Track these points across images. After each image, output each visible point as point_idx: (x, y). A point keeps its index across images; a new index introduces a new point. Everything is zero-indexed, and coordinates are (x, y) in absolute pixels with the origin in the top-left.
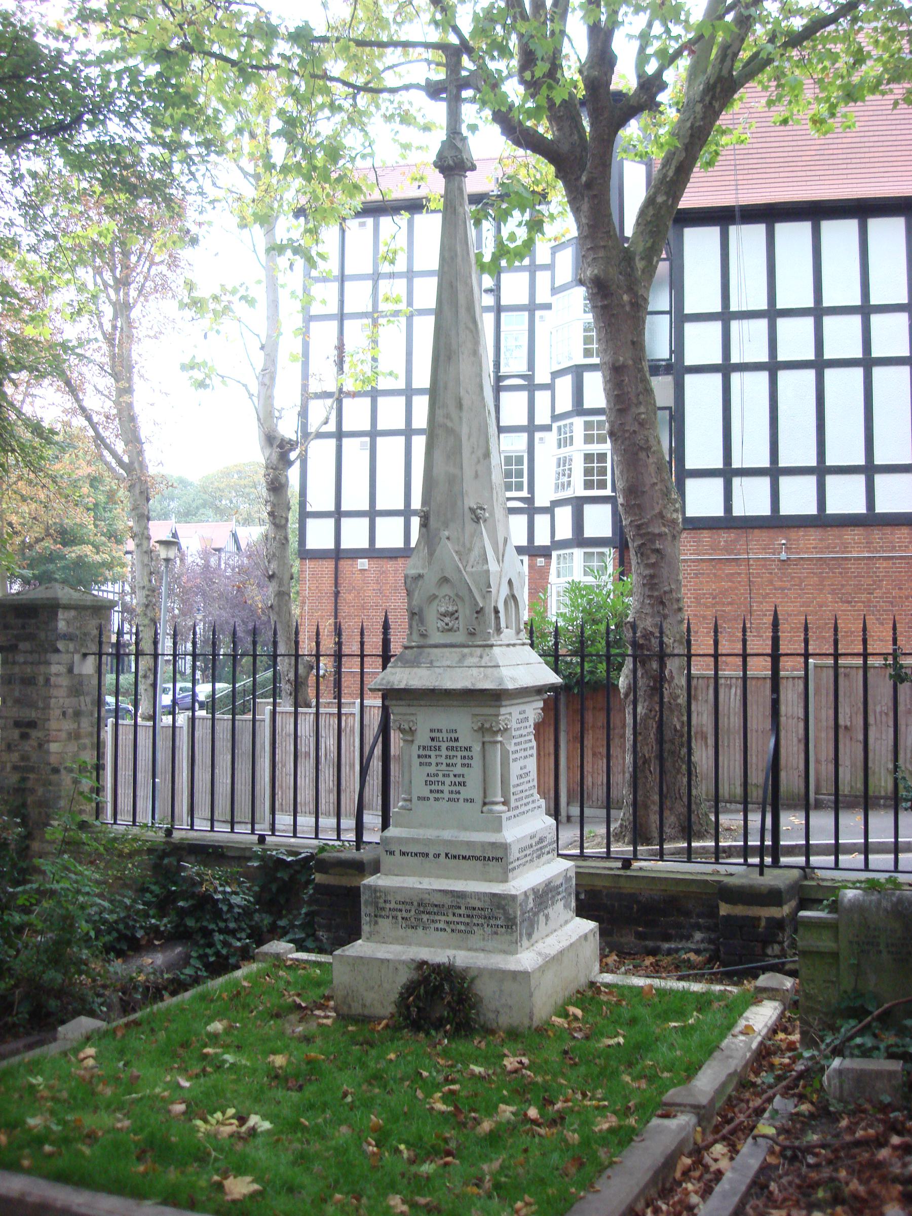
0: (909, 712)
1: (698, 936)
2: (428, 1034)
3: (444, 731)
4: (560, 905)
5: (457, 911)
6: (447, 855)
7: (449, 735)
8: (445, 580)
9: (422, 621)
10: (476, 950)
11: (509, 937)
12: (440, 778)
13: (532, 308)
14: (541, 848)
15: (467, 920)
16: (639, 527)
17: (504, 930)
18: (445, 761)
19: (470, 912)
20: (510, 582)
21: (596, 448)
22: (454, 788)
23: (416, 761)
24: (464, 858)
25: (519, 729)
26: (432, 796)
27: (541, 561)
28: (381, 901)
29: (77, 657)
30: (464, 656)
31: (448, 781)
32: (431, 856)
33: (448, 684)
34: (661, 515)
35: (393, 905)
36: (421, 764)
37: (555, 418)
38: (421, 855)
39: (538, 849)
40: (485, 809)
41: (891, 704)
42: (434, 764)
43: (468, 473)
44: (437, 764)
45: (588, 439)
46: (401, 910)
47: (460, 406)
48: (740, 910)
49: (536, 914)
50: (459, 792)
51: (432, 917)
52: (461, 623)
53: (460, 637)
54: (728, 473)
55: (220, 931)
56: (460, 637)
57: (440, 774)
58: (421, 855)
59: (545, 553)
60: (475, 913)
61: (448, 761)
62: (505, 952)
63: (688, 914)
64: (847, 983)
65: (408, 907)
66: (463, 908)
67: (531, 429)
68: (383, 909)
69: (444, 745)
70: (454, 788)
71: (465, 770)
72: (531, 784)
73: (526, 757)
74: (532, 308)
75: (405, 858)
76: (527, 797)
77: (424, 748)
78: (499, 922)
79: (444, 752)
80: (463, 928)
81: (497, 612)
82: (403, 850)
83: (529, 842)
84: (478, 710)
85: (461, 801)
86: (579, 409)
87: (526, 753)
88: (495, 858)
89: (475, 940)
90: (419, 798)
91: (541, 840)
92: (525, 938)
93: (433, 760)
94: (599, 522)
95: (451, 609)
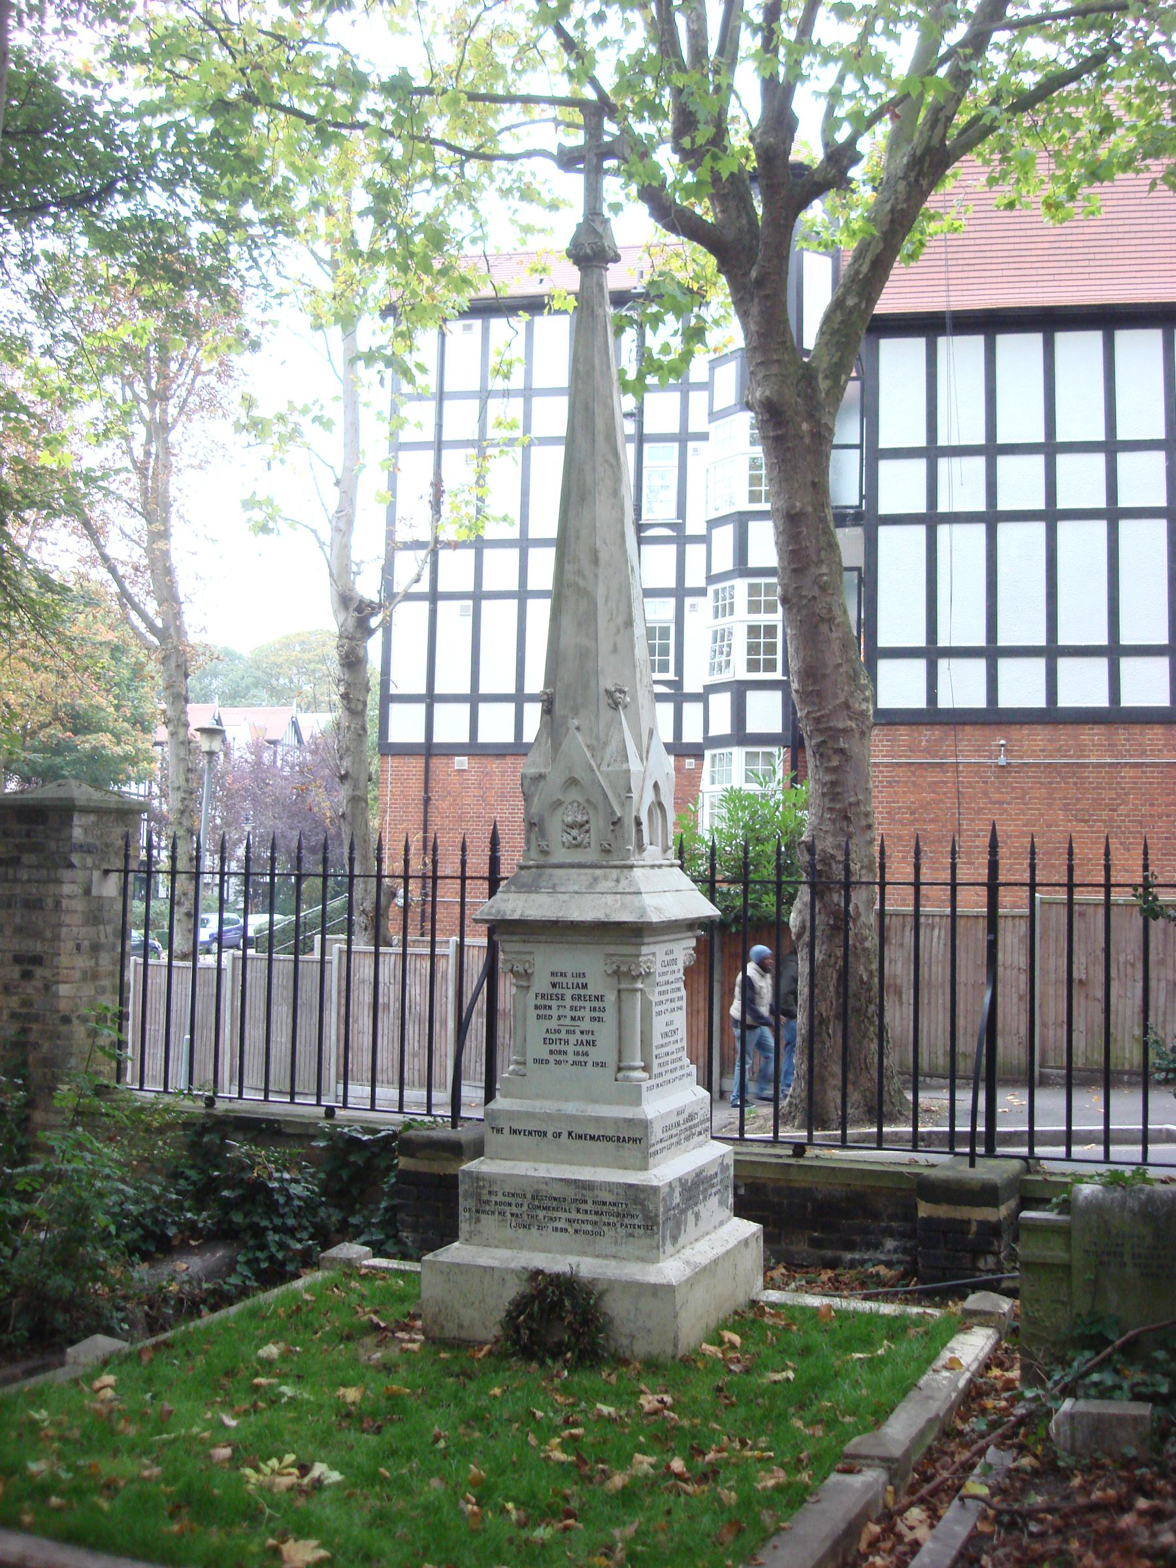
0: (1162, 962)
1: (890, 1244)
2: (542, 1363)
4: (714, 1201)
5: (583, 1207)
6: (570, 1134)
7: (575, 981)
8: (572, 782)
9: (542, 833)
10: (606, 1257)
11: (649, 1241)
12: (563, 1035)
13: (683, 438)
14: (691, 1128)
15: (595, 1218)
16: (818, 720)
17: (642, 1231)
18: (569, 1014)
19: (599, 1208)
20: (656, 786)
21: (763, 619)
22: (580, 1049)
23: (532, 1013)
24: (592, 1138)
25: (664, 974)
26: (552, 1058)
27: (690, 763)
28: (485, 1192)
29: (96, 875)
30: (596, 879)
31: (572, 1039)
32: (549, 1135)
33: (576, 915)
34: (847, 706)
36: (539, 1017)
37: (711, 579)
38: (537, 1134)
39: (687, 1128)
40: (620, 1075)
41: (1139, 953)
43: (604, 646)
44: (559, 1018)
45: (754, 607)
46: (510, 1204)
47: (596, 561)
48: (943, 1211)
49: (683, 1212)
50: (587, 1054)
52: (593, 838)
53: (590, 855)
54: (932, 653)
55: (276, 1230)
56: (590, 855)
57: (564, 1030)
58: (537, 1134)
59: (696, 751)
60: (605, 1208)
61: (574, 1013)
62: (643, 1260)
63: (876, 1216)
64: (1082, 1304)
65: (520, 1201)
66: (590, 1202)
67: (680, 592)
68: (488, 1202)
69: (569, 993)
70: (580, 1049)
71: (595, 1026)
72: (679, 1045)
73: (673, 1010)
74: (683, 438)
76: (673, 1061)
77: (543, 996)
78: (636, 1222)
79: (568, 1002)
80: (589, 1228)
81: (638, 823)
83: (674, 1119)
84: (612, 949)
85: (590, 1064)
86: (742, 568)
87: (674, 1005)
88: (632, 1139)
89: (604, 1243)
90: (536, 1061)
91: (691, 1117)
92: (668, 1242)
93: (554, 1013)
94: (766, 713)
95: (580, 818)
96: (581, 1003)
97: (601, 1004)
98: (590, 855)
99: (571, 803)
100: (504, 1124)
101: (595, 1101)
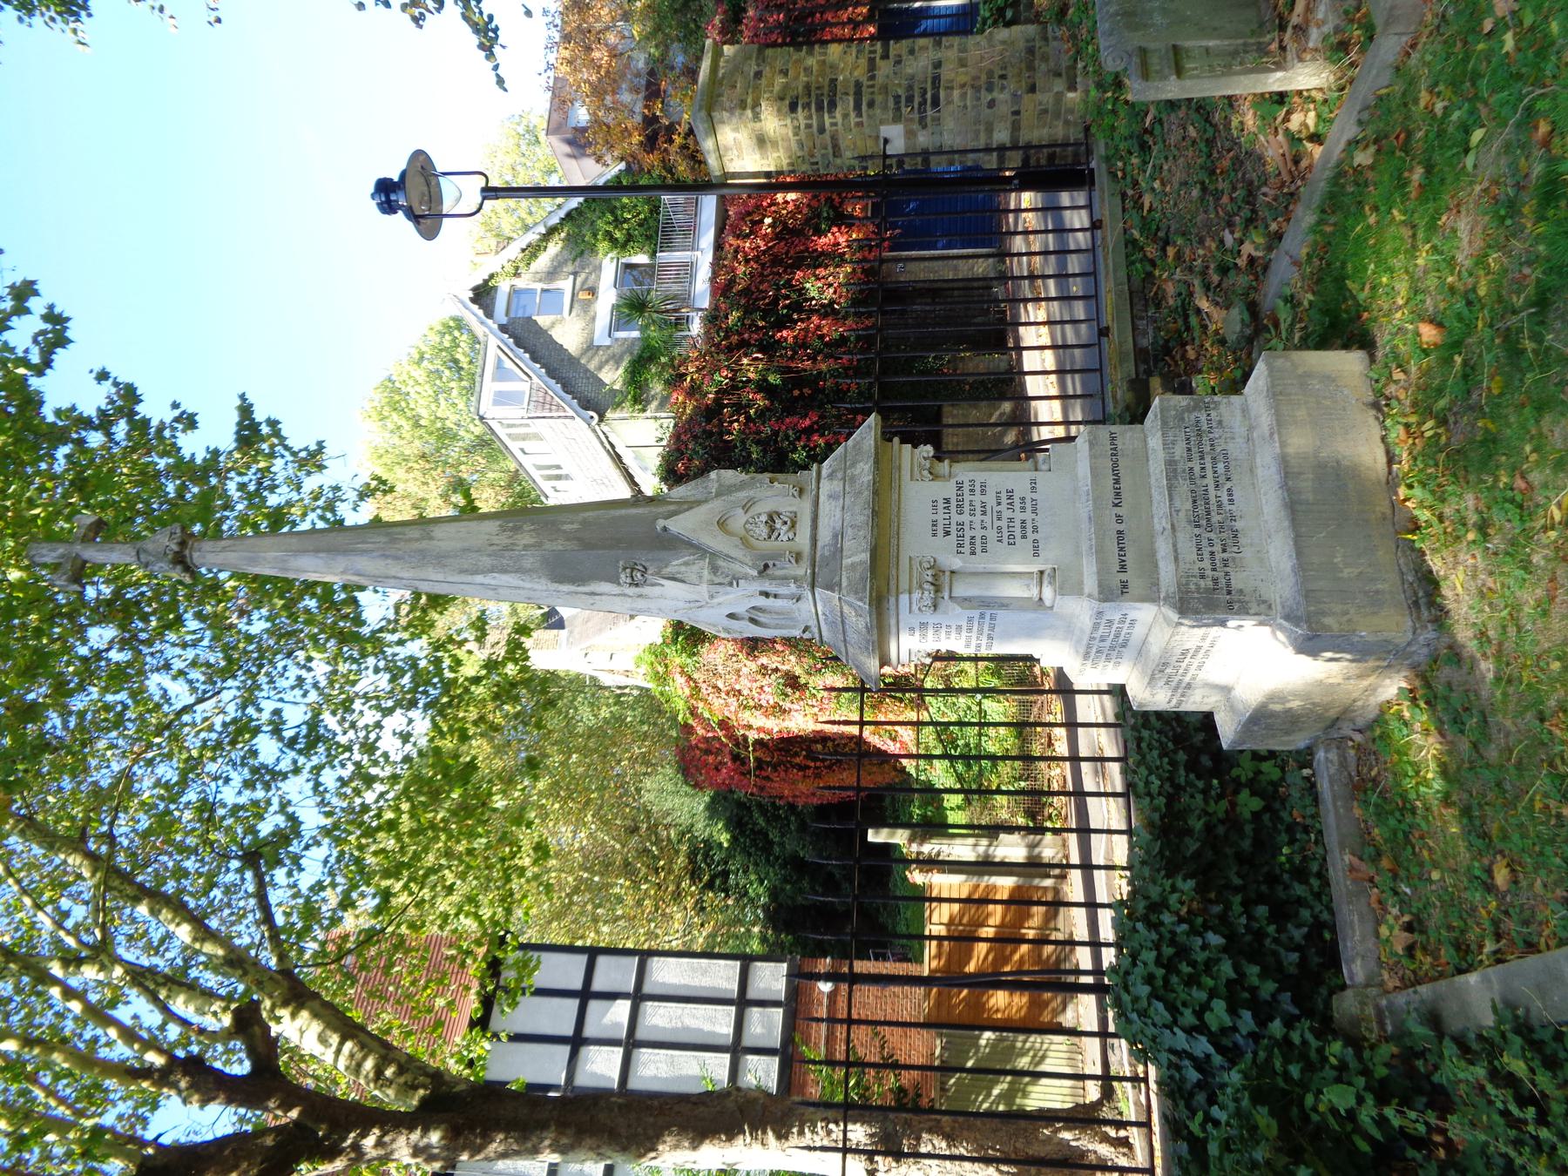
3: (935, 517)
5: (1197, 469)
6: (1116, 505)
12: (1004, 523)
15: (1208, 459)
17: (1213, 414)
18: (978, 517)
19: (1196, 456)
24: (1117, 481)
28: (1202, 583)
31: (1007, 514)
32: (1121, 527)
35: (1207, 564)
36: (984, 551)
42: (983, 532)
46: (1212, 553)
50: (1023, 499)
51: (1213, 507)
54: (737, 1049)
60: (1195, 450)
61: (978, 512)
65: (1205, 543)
66: (1190, 464)
75: (1129, 564)
78: (1203, 418)
79: (966, 518)
80: (1221, 466)
85: (1034, 496)
89: (1236, 449)
93: (978, 533)
96: (966, 504)
98: (805, 507)
99: (747, 531)
100: (1116, 579)
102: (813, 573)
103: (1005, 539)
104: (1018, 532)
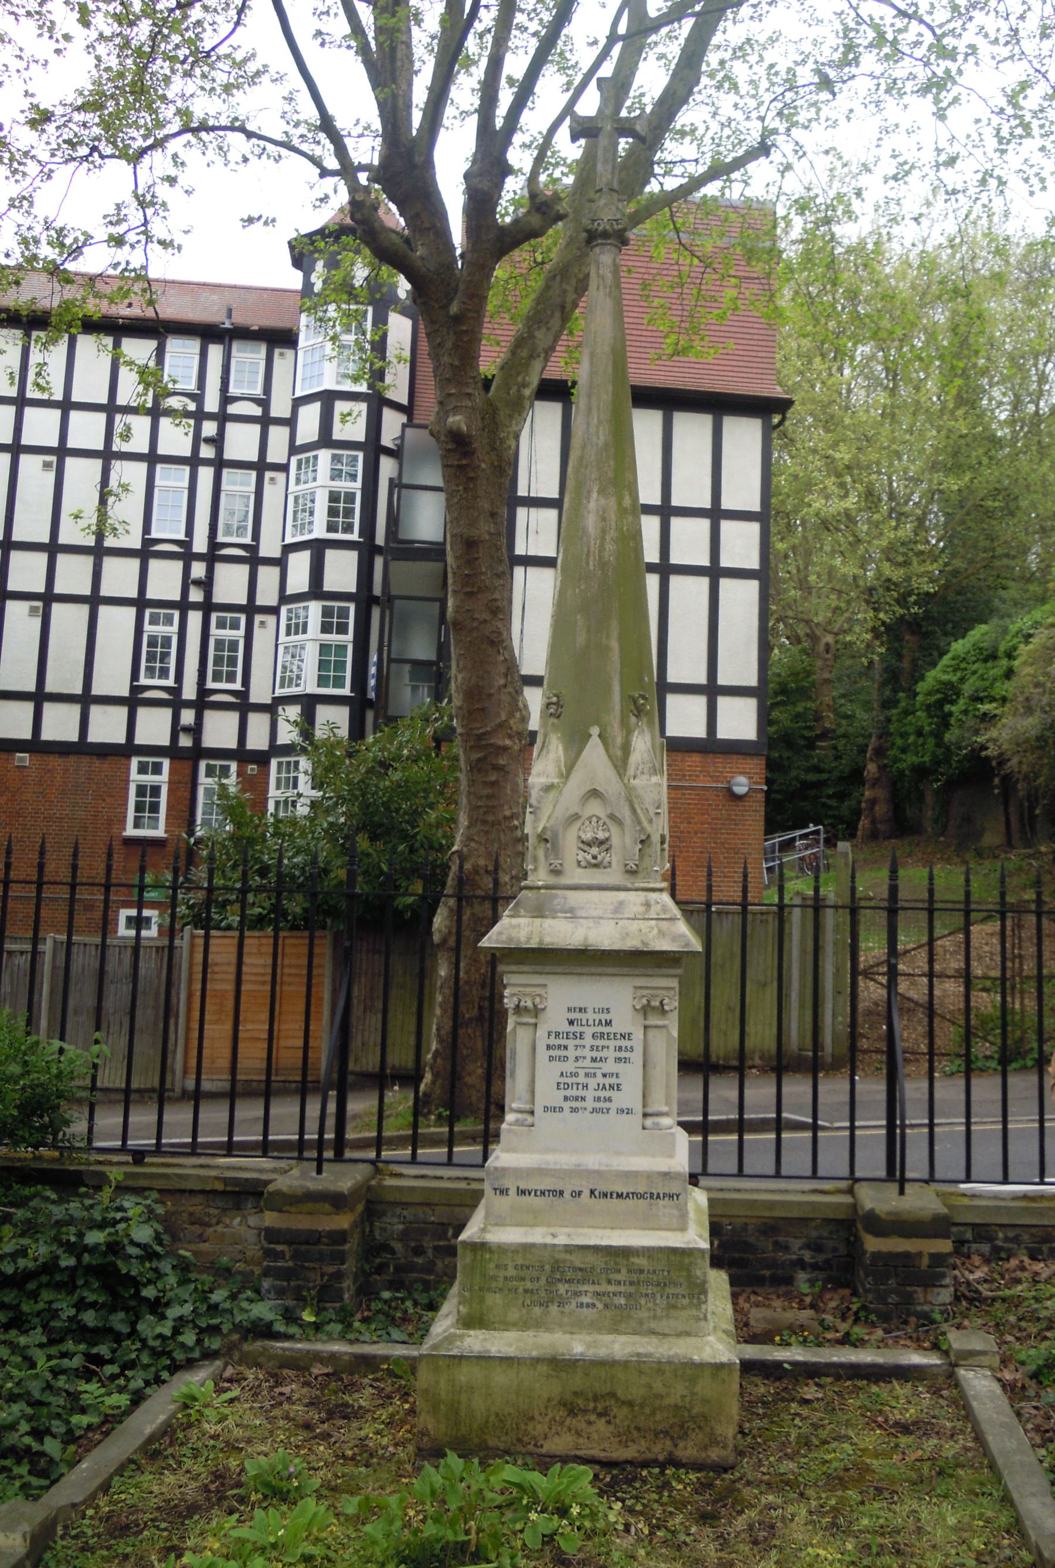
3: (590, 1011)
5: (618, 1277)
6: (592, 1192)
7: (597, 1017)
11: (694, 1312)
12: (581, 1079)
18: (589, 1054)
19: (635, 1277)
22: (602, 1094)
24: (620, 1196)
28: (492, 1265)
31: (592, 1083)
32: (567, 1195)
35: (511, 1272)
36: (551, 1058)
37: (284, 598)
40: (649, 1122)
42: (572, 1058)
44: (577, 1059)
45: (326, 628)
46: (523, 1279)
51: (574, 1287)
52: (615, 858)
56: (614, 876)
57: (582, 1072)
59: (261, 759)
61: (595, 1054)
65: (535, 1274)
67: (251, 609)
68: (494, 1278)
69: (589, 1031)
70: (602, 1094)
74: (261, 466)
77: (557, 1034)
79: (588, 1041)
82: (522, 1187)
85: (613, 1112)
86: (316, 590)
90: (546, 1109)
93: (571, 1053)
95: (601, 835)
97: (628, 1043)
99: (590, 819)
100: (511, 1184)
101: (618, 1153)
102: (539, 888)
103: (562, 1080)
104: (573, 1092)
